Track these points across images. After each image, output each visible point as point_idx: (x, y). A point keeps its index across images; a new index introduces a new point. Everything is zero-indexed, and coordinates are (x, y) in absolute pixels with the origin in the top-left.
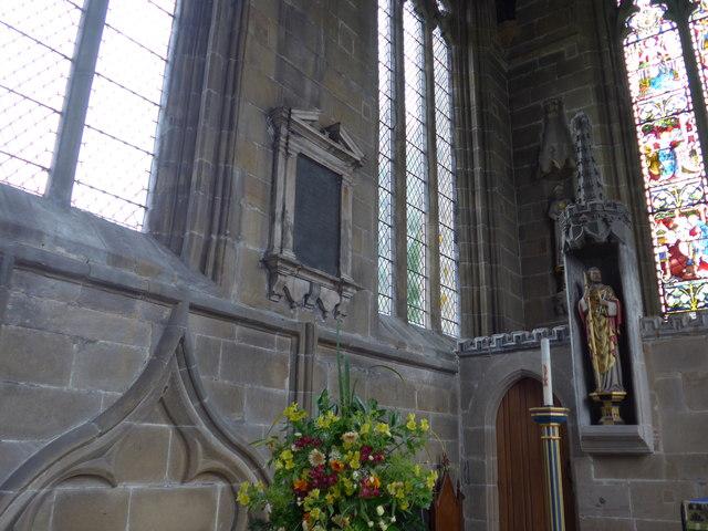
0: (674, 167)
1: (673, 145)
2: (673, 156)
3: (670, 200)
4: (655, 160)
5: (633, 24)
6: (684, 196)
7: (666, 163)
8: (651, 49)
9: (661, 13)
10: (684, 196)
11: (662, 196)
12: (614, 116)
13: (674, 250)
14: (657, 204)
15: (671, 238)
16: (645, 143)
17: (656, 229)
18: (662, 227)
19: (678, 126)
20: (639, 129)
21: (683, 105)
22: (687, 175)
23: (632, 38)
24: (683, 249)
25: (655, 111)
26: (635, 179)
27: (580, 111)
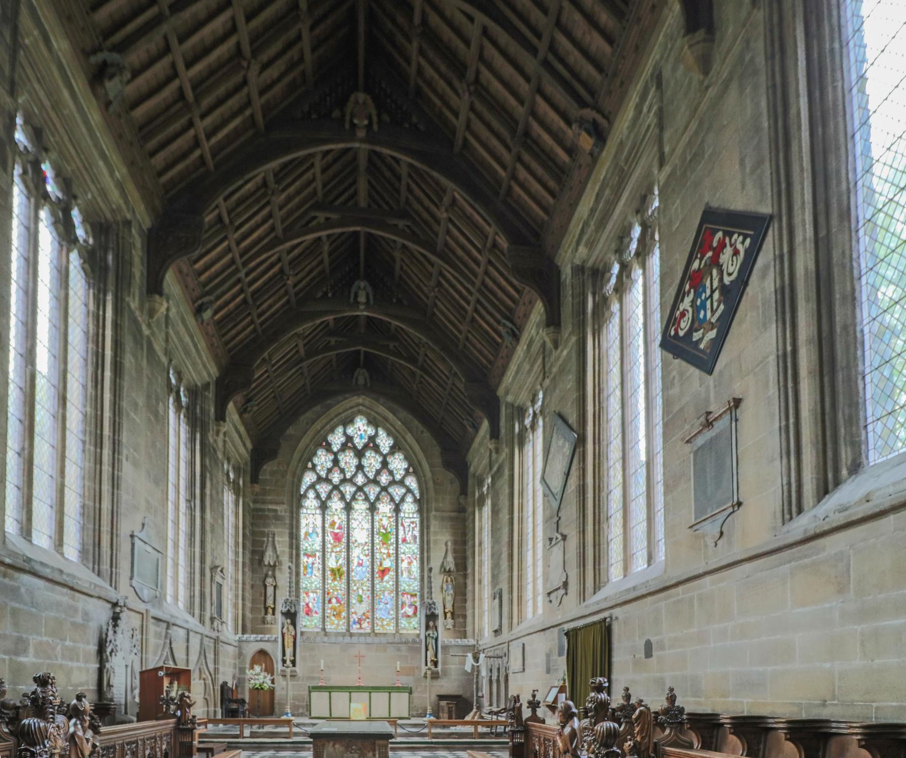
0: (312, 573)
1: (313, 564)
2: (312, 568)
3: (309, 585)
4: (306, 568)
5: (306, 504)
6: (313, 585)
7: (309, 570)
8: (311, 519)
9: (317, 505)
10: (313, 585)
11: (306, 582)
12: (294, 547)
13: (307, 605)
14: (304, 586)
15: (307, 600)
16: (304, 559)
17: (303, 595)
18: (305, 595)
19: (315, 556)
20: (302, 553)
21: (318, 548)
22: (314, 577)
23: (305, 511)
24: (310, 605)
25: (309, 548)
26: (298, 574)
27: (282, 541)
